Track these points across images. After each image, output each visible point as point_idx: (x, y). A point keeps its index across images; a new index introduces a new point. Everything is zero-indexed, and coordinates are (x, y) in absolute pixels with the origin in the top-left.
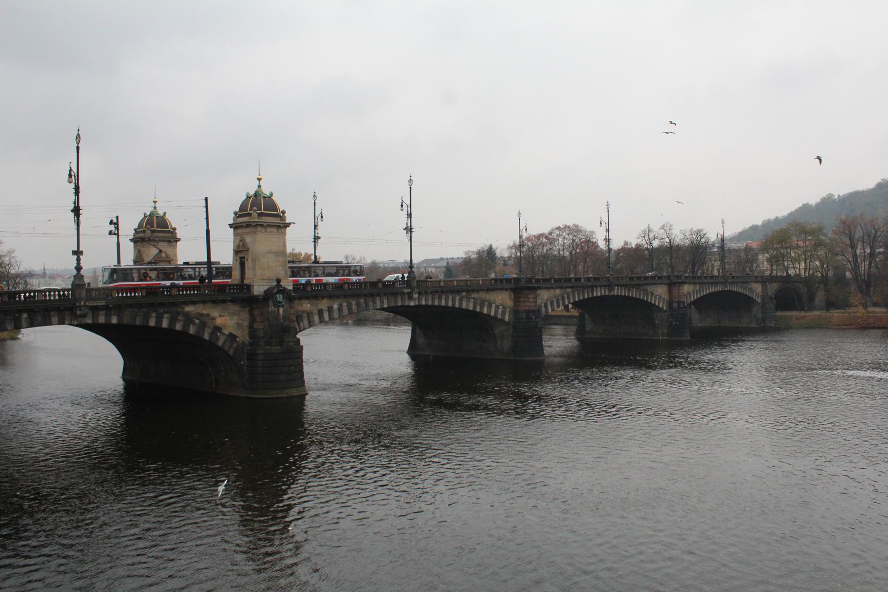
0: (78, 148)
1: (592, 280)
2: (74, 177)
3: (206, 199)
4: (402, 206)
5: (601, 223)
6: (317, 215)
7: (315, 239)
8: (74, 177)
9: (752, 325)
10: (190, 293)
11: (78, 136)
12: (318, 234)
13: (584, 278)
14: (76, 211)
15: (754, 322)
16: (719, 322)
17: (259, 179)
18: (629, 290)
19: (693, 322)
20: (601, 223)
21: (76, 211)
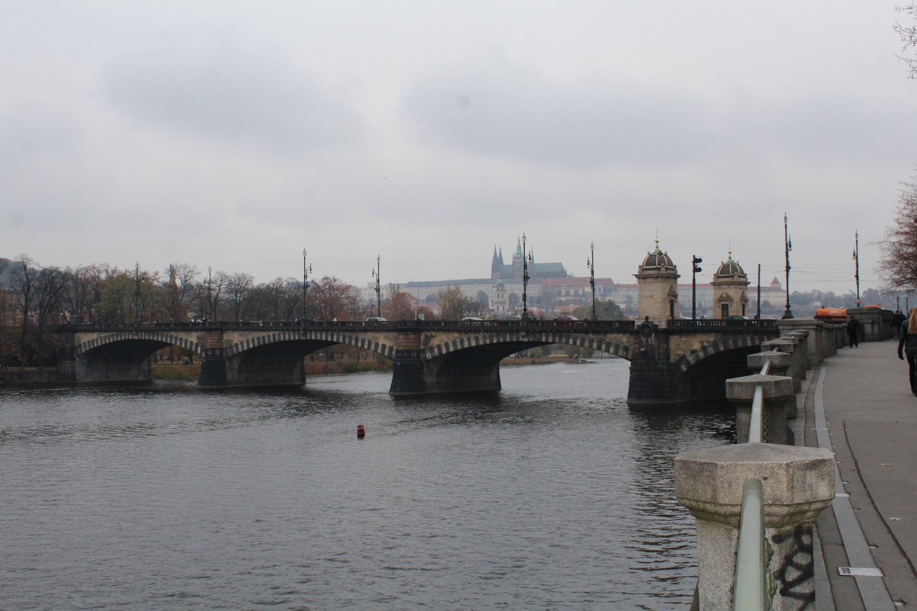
0: (857, 241)
1: (316, 324)
2: (856, 256)
3: (759, 265)
4: (588, 264)
5: (373, 274)
6: (526, 256)
7: (524, 278)
8: (856, 256)
9: (140, 378)
10: (715, 325)
11: (857, 235)
12: (527, 273)
13: (273, 323)
14: (857, 276)
15: (142, 375)
16: (107, 377)
17: (730, 253)
18: (158, 335)
19: (78, 377)
20: (373, 274)
21: (857, 276)
